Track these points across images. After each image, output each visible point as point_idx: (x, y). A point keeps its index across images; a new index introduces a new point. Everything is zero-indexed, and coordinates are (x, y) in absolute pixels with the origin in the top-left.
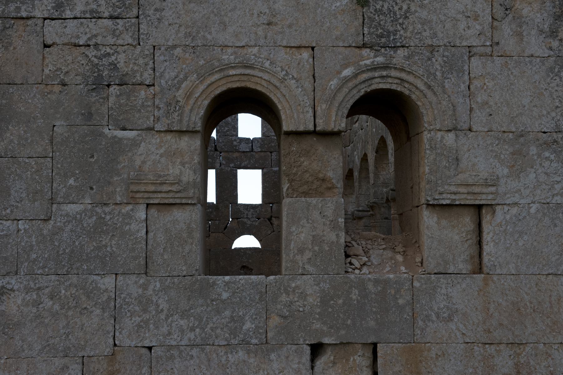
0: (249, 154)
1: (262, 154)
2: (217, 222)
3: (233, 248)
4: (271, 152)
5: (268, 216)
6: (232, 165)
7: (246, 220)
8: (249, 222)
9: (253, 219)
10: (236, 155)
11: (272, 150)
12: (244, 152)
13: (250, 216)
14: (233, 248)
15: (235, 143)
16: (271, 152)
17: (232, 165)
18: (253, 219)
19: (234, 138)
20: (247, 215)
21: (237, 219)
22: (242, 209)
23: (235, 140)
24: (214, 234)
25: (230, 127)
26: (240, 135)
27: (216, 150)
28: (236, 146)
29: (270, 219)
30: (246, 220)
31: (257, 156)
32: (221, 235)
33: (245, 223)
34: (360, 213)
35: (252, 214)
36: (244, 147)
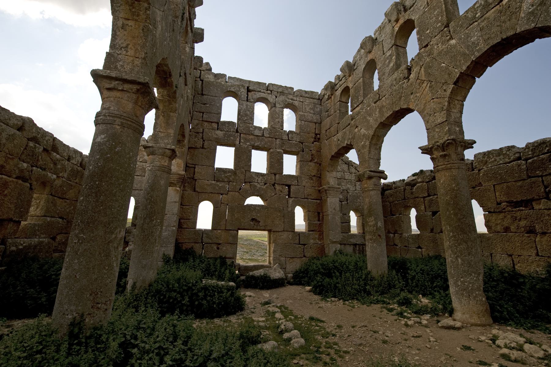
0: (261, 138)
1: (270, 139)
2: (234, 184)
3: (245, 204)
4: (276, 139)
5: (273, 183)
6: (248, 144)
7: (256, 184)
8: (259, 186)
9: (261, 184)
10: (251, 137)
11: (277, 137)
12: (257, 136)
13: (259, 181)
14: (245, 204)
15: (251, 129)
16: (276, 139)
17: (248, 144)
18: (261, 184)
19: (250, 125)
20: (258, 180)
21: (250, 182)
22: (254, 176)
23: (252, 127)
24: (231, 193)
25: (249, 118)
26: (255, 124)
27: (237, 132)
28: (252, 131)
29: (274, 185)
30: (256, 184)
31: (266, 140)
32: (237, 193)
33: (256, 186)
34: (372, 173)
35: (261, 180)
36: (257, 133)
